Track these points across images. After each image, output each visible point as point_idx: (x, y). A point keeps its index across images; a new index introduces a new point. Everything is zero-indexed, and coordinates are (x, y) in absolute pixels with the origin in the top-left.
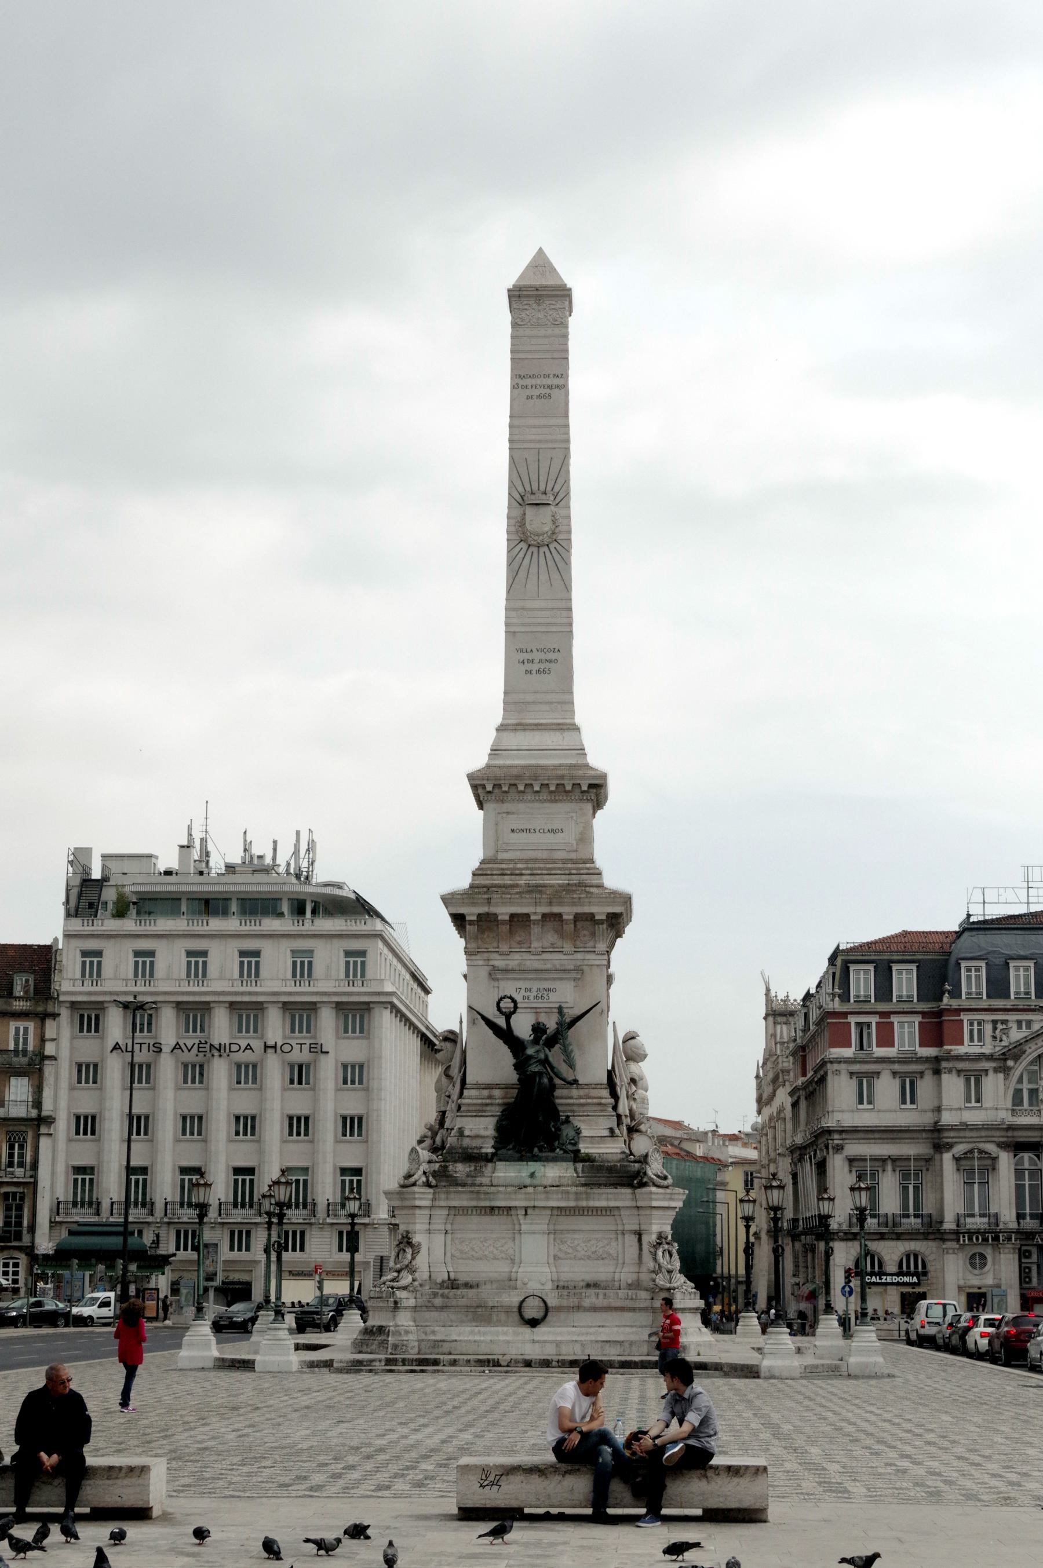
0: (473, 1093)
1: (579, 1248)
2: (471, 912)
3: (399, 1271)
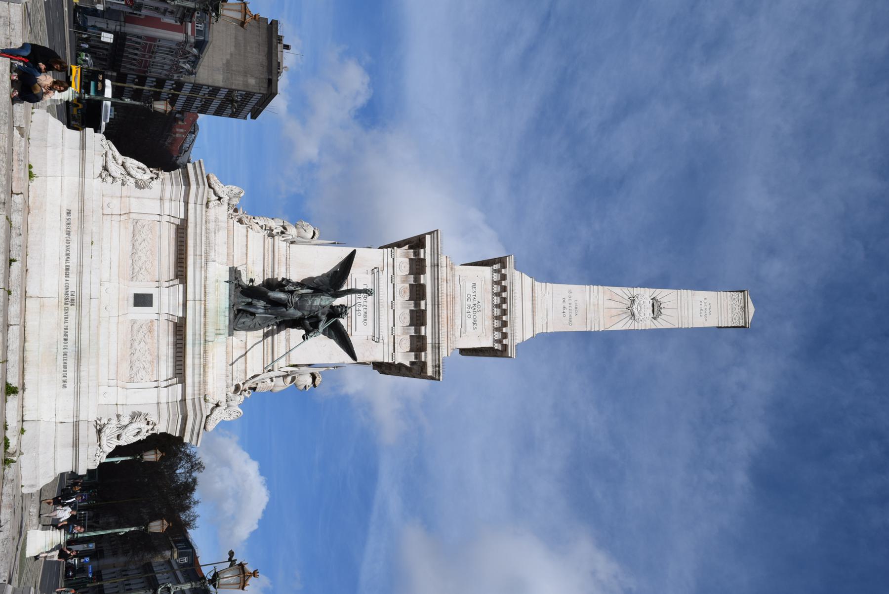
0: (283, 251)
1: (143, 344)
2: (426, 254)
3: (123, 165)
